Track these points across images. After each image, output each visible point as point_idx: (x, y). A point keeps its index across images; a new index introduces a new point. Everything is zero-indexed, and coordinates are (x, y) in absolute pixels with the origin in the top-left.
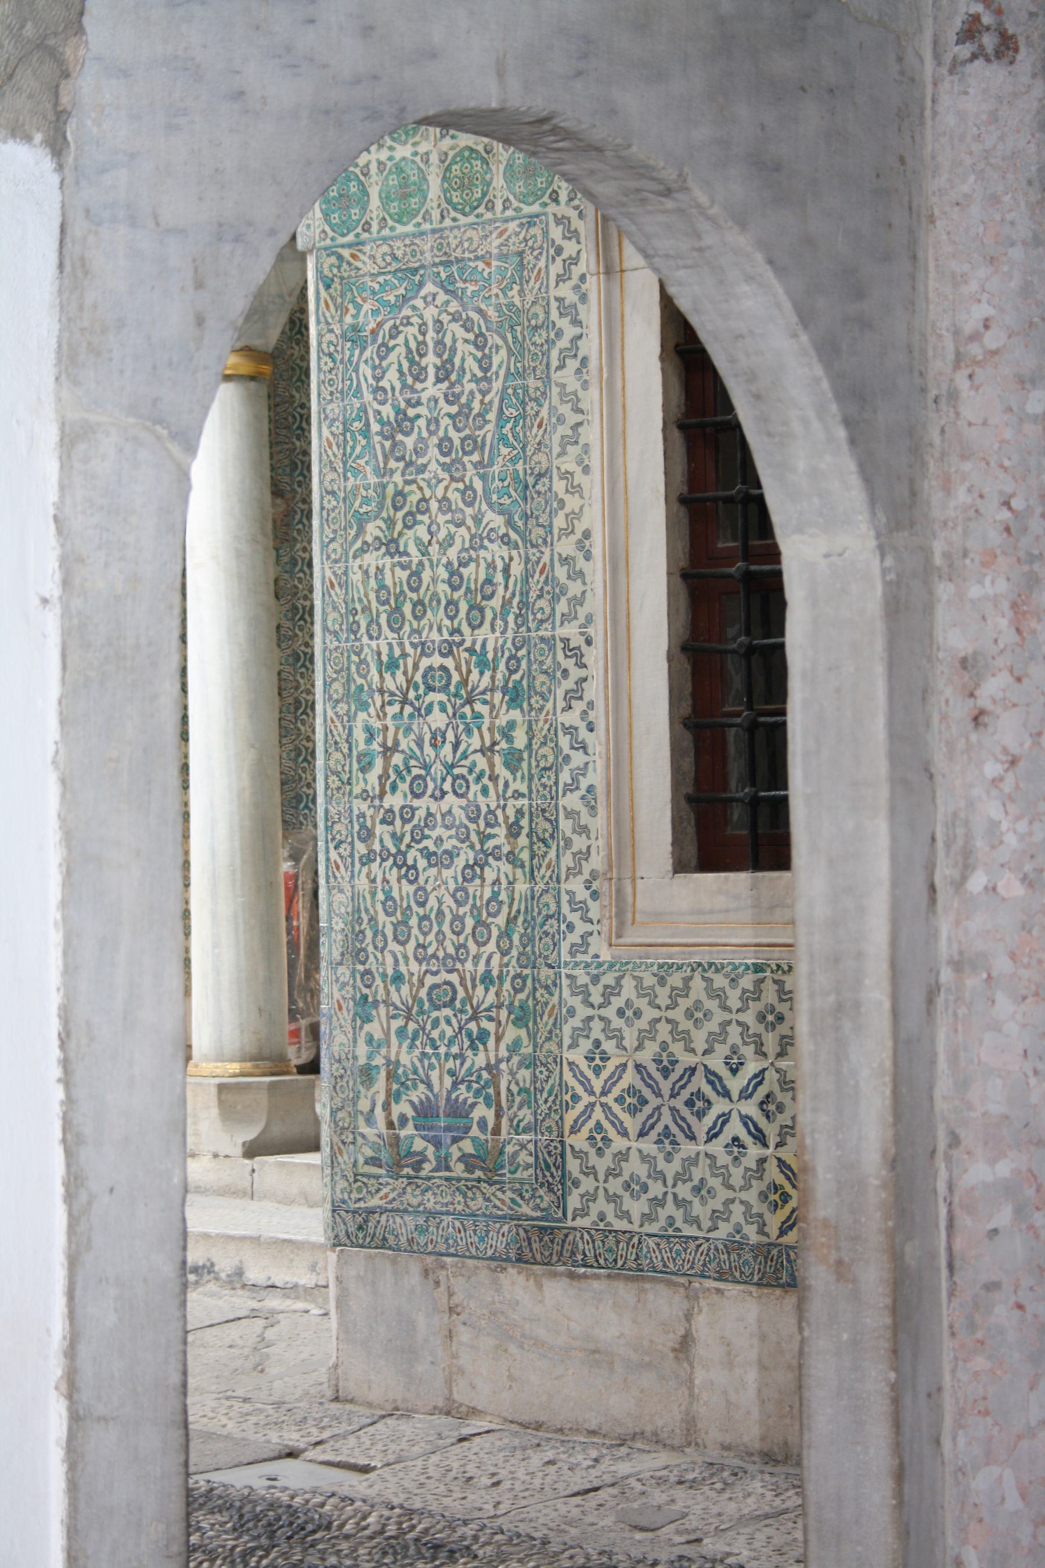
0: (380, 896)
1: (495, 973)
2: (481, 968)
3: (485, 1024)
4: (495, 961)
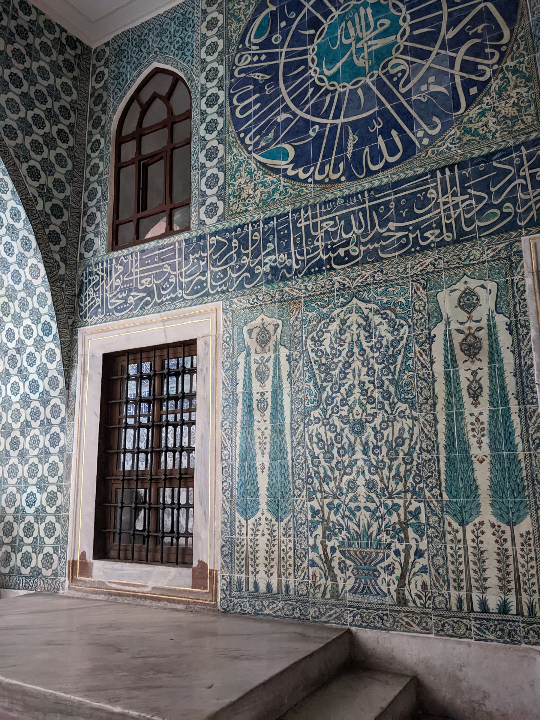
0: (315, 440)
1: (402, 474)
2: (393, 473)
3: (396, 501)
4: (402, 469)
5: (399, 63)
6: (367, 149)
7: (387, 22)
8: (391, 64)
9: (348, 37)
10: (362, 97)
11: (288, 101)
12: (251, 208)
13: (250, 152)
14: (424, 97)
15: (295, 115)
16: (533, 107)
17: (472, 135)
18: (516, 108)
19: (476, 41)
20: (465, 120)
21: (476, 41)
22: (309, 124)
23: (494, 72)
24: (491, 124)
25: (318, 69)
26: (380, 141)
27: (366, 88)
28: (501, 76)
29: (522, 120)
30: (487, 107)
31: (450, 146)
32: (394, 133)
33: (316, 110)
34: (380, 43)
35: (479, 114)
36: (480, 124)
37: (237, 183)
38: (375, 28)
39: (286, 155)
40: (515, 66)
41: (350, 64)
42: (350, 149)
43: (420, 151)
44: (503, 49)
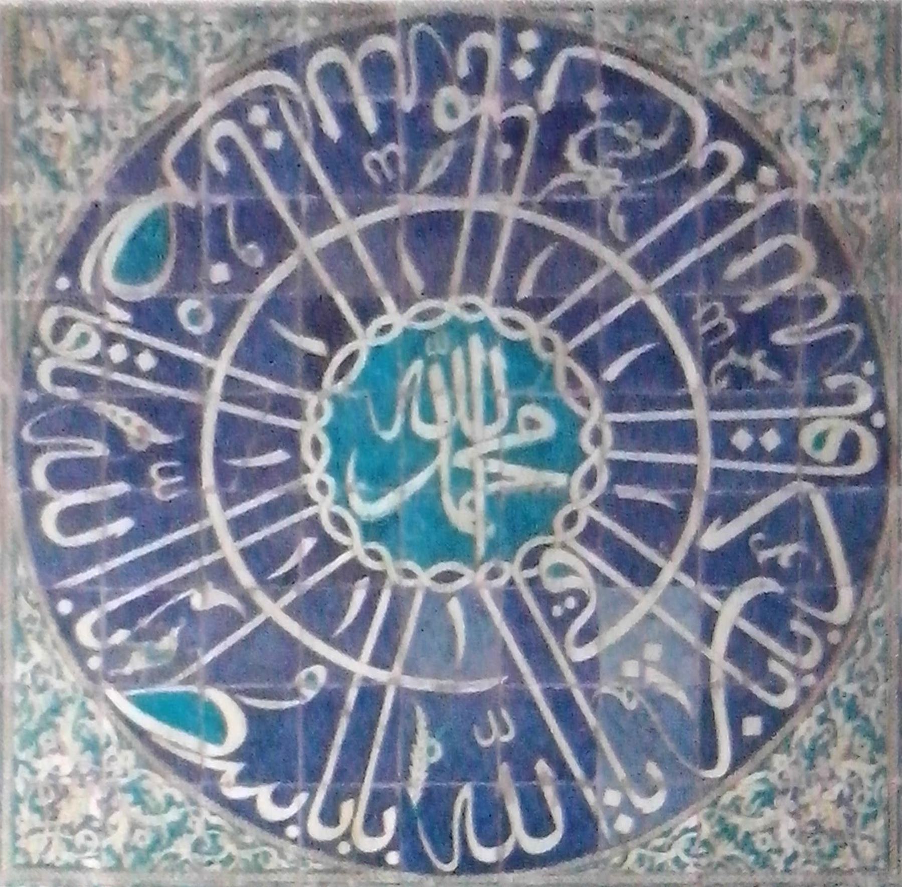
5: (573, 566)
6: (466, 793)
7: (548, 427)
8: (549, 559)
9: (429, 417)
10: (461, 628)
11: (230, 549)
12: (90, 863)
13: (92, 676)
14: (630, 695)
15: (253, 609)
16: (880, 822)
17: (738, 846)
18: (843, 810)
19: (771, 585)
20: (727, 798)
21: (771, 585)
22: (296, 657)
23: (805, 693)
24: (783, 832)
25: (330, 481)
26: (504, 781)
27: (471, 600)
28: (819, 710)
29: (854, 847)
30: (780, 785)
31: (685, 859)
32: (542, 767)
33: (319, 610)
34: (522, 477)
35: (759, 794)
36: (760, 823)
37: (44, 766)
38: (511, 427)
39: (215, 728)
40: (854, 697)
41: (428, 504)
42: (419, 775)
43: (609, 846)
44: (834, 637)
